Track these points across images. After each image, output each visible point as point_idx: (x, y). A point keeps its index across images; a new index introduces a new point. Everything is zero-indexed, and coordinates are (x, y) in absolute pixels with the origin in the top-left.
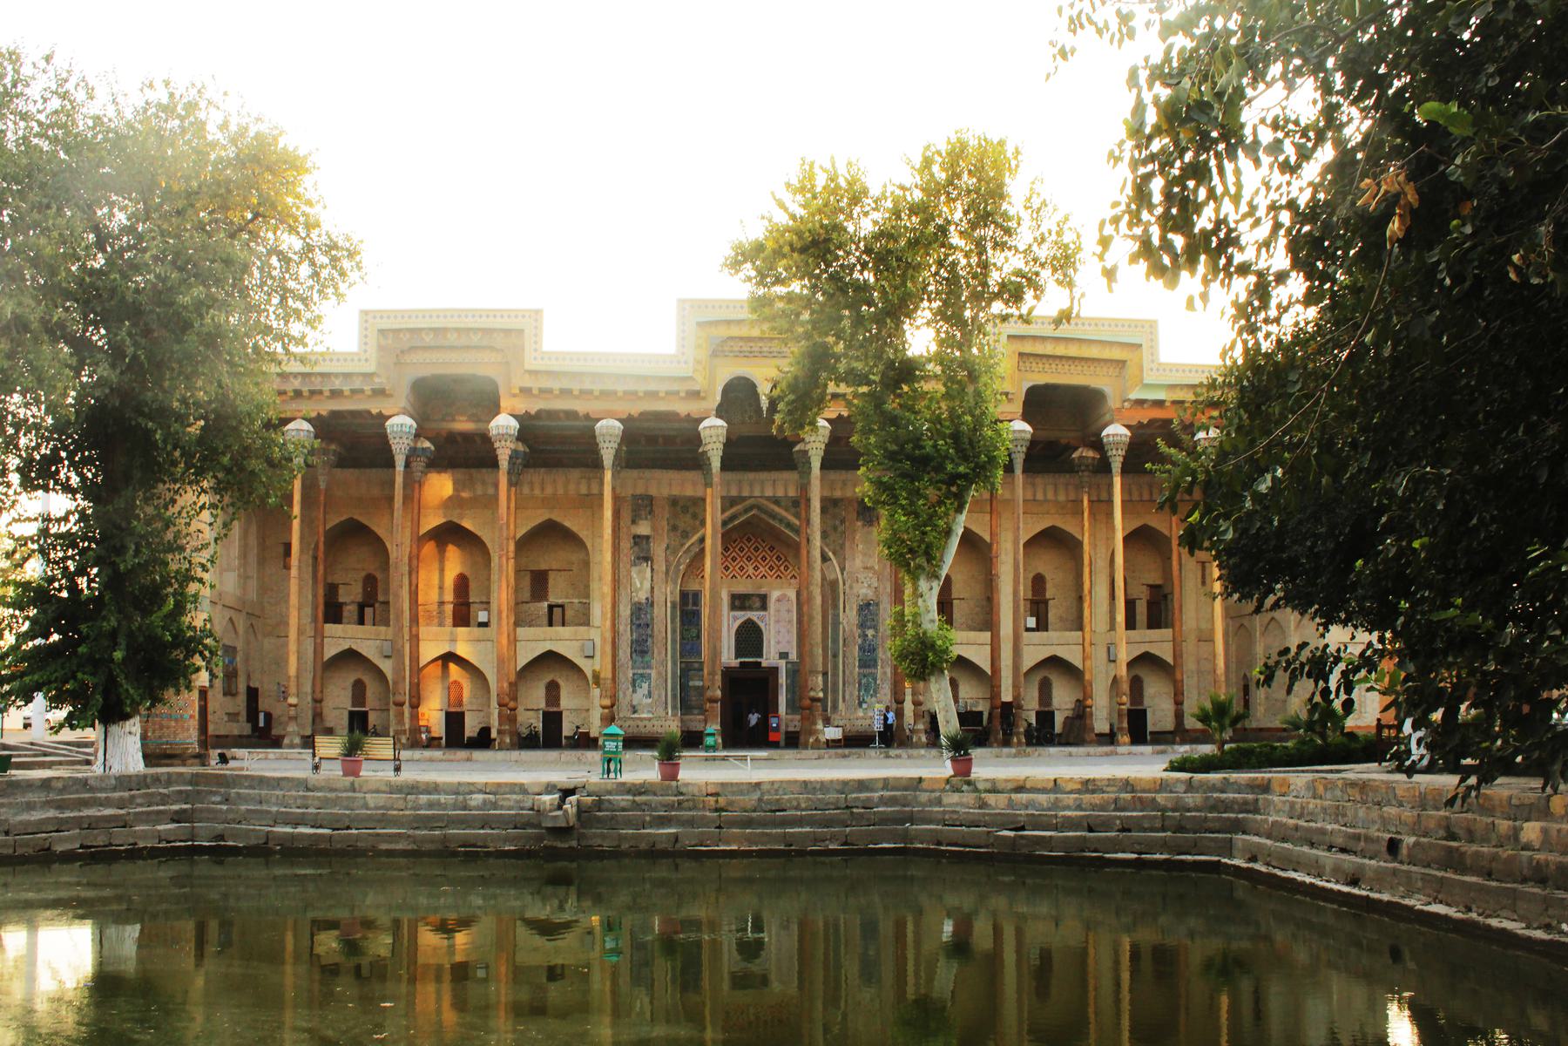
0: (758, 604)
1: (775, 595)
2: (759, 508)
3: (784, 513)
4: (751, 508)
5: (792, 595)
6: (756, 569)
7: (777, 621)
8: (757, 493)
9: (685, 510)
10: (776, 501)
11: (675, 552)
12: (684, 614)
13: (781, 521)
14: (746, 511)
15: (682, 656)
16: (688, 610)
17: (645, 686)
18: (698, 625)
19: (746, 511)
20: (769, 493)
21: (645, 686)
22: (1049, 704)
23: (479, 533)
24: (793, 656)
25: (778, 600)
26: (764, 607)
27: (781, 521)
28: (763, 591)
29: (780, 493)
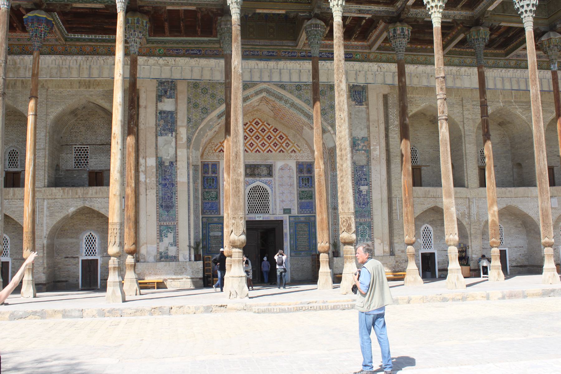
0: (265, 172)
1: (278, 165)
2: (268, 91)
3: (288, 95)
4: (261, 91)
5: (293, 165)
7: (281, 185)
8: (266, 79)
9: (205, 91)
10: (283, 86)
12: (205, 180)
13: (286, 101)
15: (203, 213)
16: (208, 179)
19: (257, 94)
20: (276, 78)
26: (270, 174)
28: (269, 162)
29: (285, 79)
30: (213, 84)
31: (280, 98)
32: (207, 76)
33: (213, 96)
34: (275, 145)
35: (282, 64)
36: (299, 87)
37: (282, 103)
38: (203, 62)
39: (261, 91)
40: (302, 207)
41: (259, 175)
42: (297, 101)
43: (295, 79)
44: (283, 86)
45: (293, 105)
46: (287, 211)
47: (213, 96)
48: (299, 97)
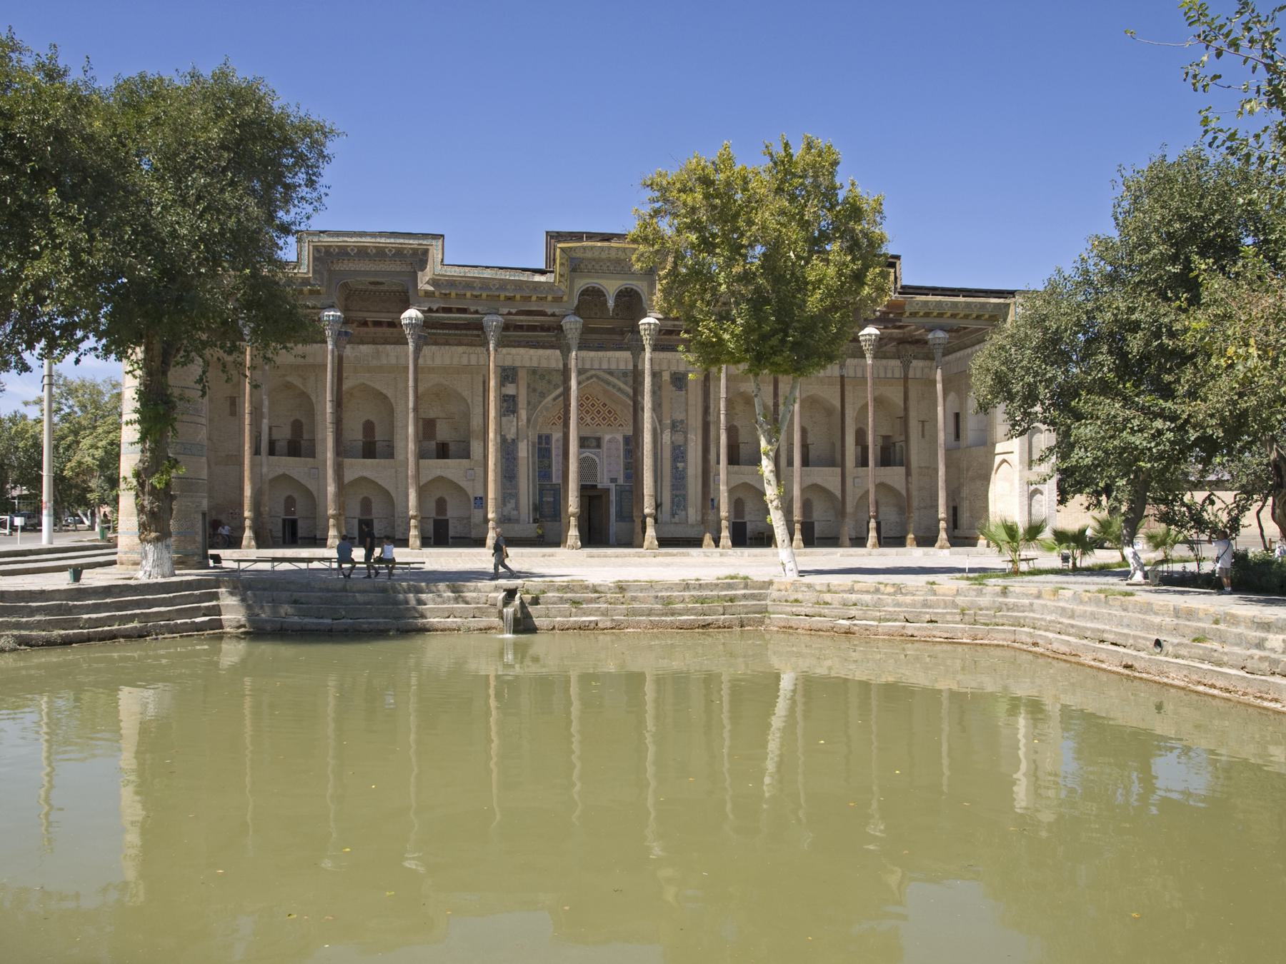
0: (594, 444)
1: (607, 437)
2: (598, 377)
4: (591, 377)
5: (621, 439)
6: (593, 419)
8: (596, 366)
9: (542, 377)
10: (611, 373)
11: (535, 408)
13: (614, 386)
14: (588, 379)
17: (513, 501)
18: (550, 457)
20: (605, 366)
21: (513, 501)
22: (811, 517)
23: (385, 391)
24: (621, 481)
25: (610, 441)
26: (599, 446)
27: (614, 386)
28: (598, 435)
29: (613, 367)
30: (550, 371)
31: (608, 383)
32: (544, 364)
33: (549, 382)
34: (604, 419)
35: (610, 354)
36: (625, 374)
37: (610, 388)
38: (541, 352)
39: (591, 377)
40: (628, 477)
41: (589, 447)
42: (623, 386)
43: (622, 367)
44: (611, 373)
45: (620, 389)
46: (613, 480)
47: (549, 382)
48: (626, 383)
